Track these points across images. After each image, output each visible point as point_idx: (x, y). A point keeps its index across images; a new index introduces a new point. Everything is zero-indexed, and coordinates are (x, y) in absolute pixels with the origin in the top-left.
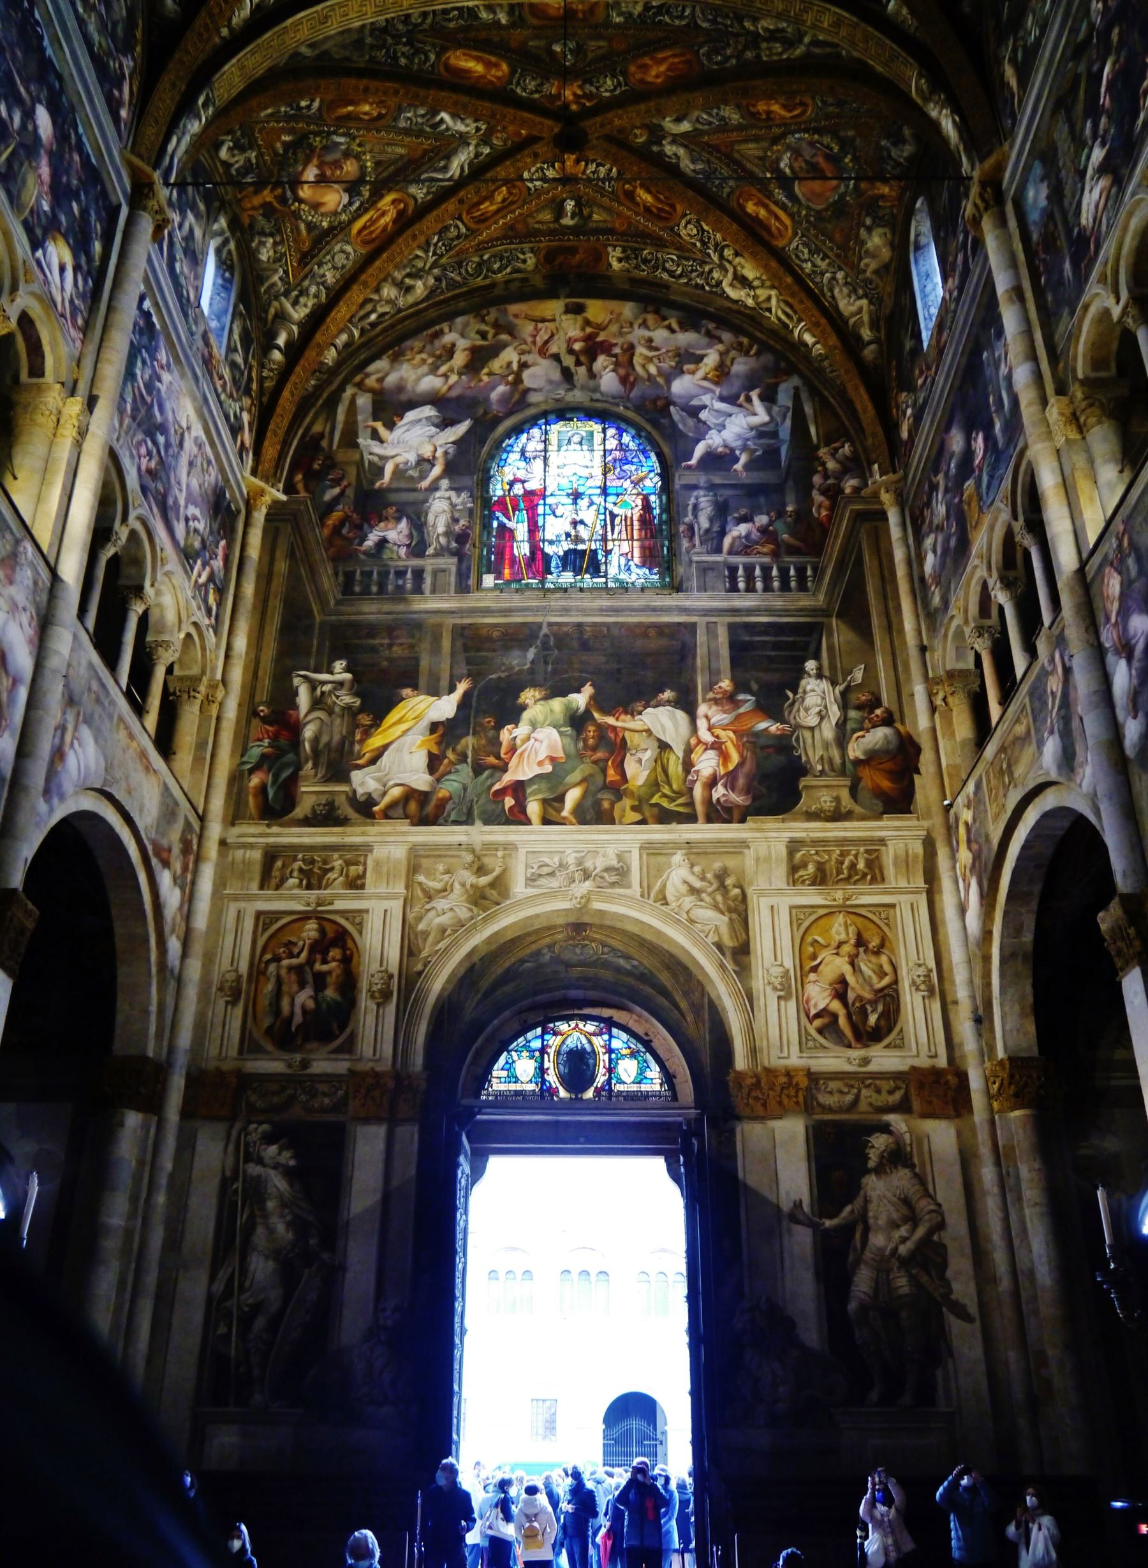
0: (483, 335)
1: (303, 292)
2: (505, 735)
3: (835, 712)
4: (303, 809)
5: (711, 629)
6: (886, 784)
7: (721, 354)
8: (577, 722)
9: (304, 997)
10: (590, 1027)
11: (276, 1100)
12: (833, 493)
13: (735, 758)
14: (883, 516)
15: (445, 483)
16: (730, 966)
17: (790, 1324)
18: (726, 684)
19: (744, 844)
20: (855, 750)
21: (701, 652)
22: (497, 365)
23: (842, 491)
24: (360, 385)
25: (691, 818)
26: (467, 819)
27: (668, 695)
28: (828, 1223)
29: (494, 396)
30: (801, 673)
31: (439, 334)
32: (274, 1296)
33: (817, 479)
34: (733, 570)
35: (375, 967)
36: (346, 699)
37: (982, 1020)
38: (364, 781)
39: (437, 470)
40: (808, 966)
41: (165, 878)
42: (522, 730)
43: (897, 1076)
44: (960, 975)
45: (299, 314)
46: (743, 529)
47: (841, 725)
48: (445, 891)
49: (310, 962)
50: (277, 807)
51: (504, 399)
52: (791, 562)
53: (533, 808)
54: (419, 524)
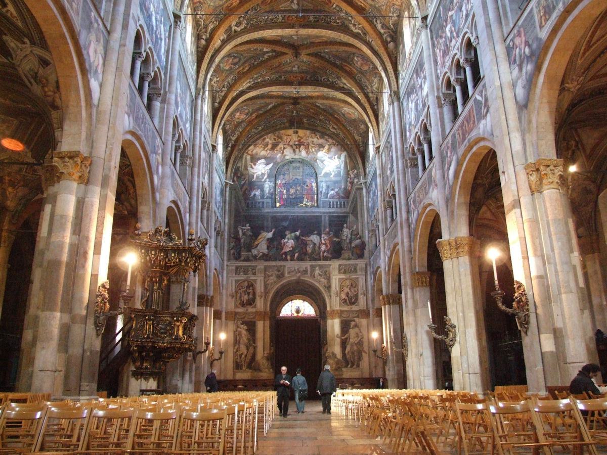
0: (275, 139)
1: (235, 134)
2: (282, 241)
3: (349, 236)
4: (242, 258)
5: (325, 216)
6: (359, 252)
7: (330, 145)
8: (297, 238)
9: (246, 297)
10: (301, 301)
11: (243, 316)
12: (352, 183)
13: (329, 247)
14: (362, 189)
15: (268, 180)
16: (327, 290)
17: (336, 355)
18: (327, 230)
19: (330, 265)
20: (353, 245)
21: (323, 222)
22: (278, 148)
23: (353, 183)
24: (247, 153)
25: (320, 260)
26: (275, 260)
27: (316, 232)
28: (343, 338)
29: (278, 156)
30: (343, 227)
31: (264, 139)
32: (245, 352)
33: (349, 179)
34: (330, 202)
35: (259, 291)
36: (250, 233)
37: (373, 301)
38: (254, 252)
39: (266, 177)
40: (341, 290)
41: (220, 276)
42: (286, 240)
43: (357, 311)
44: (370, 292)
45: (234, 139)
46: (332, 192)
47: (351, 239)
48: (272, 275)
49: (246, 290)
50: (237, 257)
51: (280, 157)
52: (342, 201)
53: (289, 258)
54: (262, 190)
